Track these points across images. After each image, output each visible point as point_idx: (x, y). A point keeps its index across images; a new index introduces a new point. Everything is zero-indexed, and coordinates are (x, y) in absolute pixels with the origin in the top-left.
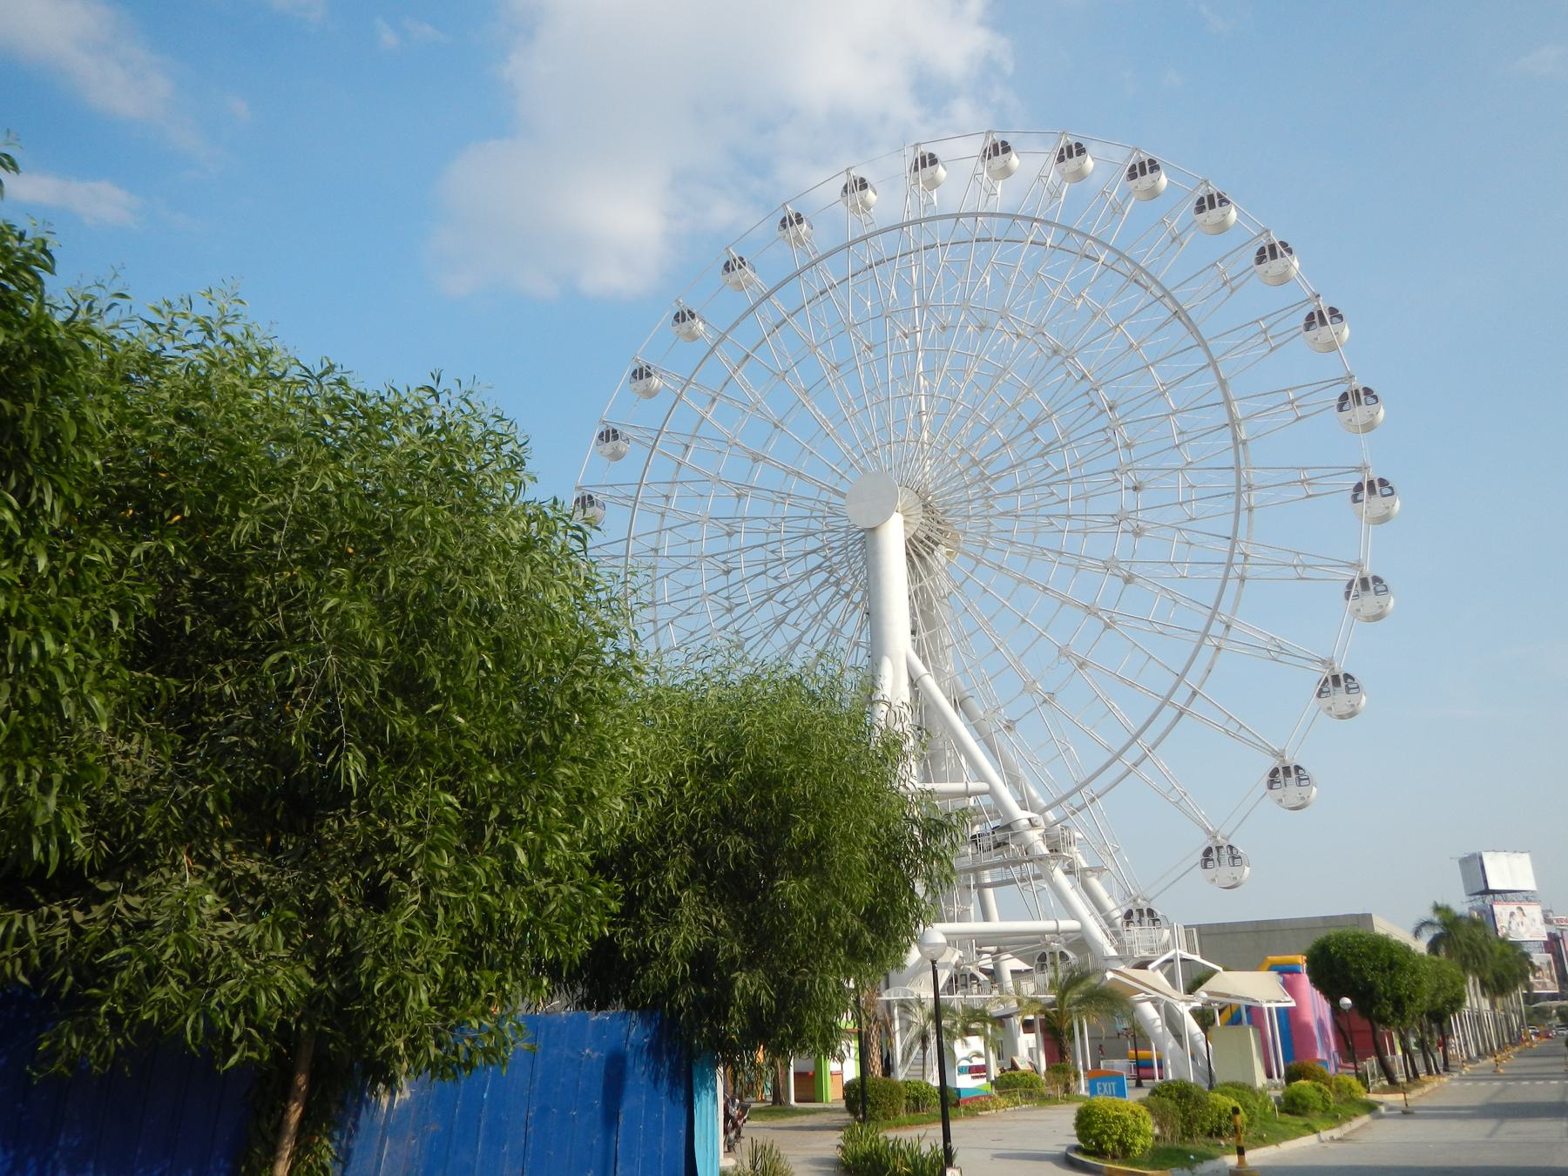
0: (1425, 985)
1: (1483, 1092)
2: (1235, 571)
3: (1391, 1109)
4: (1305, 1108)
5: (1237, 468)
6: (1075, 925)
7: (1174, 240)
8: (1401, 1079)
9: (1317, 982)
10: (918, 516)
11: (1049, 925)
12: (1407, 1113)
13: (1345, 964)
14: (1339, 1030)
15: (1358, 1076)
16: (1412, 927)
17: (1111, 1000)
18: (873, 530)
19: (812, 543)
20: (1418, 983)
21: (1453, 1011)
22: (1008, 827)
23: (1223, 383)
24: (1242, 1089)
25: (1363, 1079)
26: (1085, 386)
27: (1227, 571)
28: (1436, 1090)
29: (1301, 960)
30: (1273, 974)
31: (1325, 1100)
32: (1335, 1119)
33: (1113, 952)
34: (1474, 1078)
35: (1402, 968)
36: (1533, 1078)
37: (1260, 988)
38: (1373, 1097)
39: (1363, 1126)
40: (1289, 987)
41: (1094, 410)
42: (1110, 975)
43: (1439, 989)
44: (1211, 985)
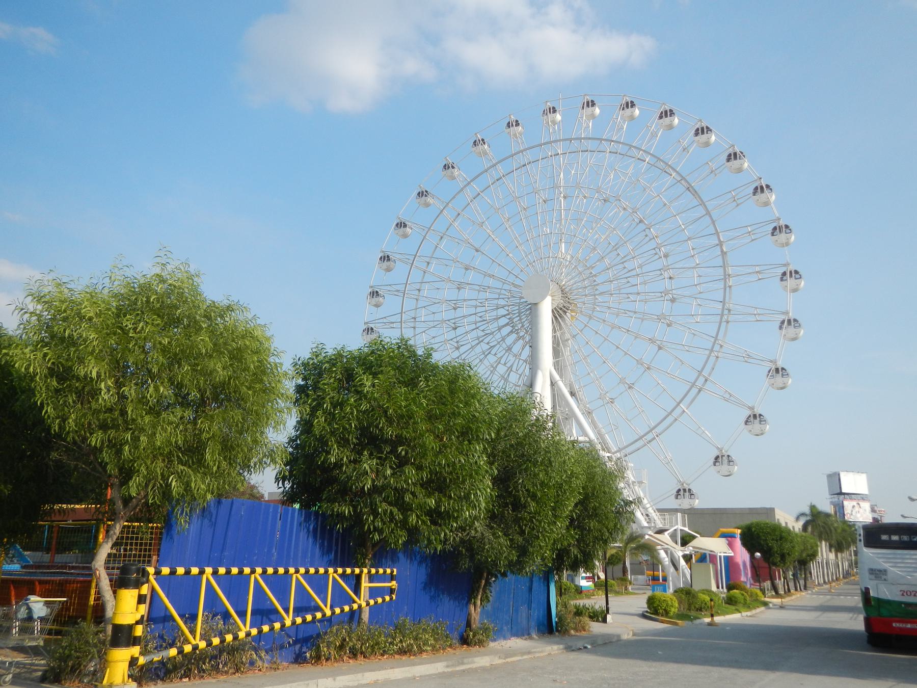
1: (821, 600)
2: (725, 315)
4: (736, 602)
5: (724, 266)
8: (781, 592)
10: (559, 295)
12: (782, 607)
13: (759, 537)
14: (753, 567)
15: (761, 590)
16: (795, 516)
18: (536, 304)
19: (502, 312)
20: (793, 547)
21: (811, 560)
23: (713, 222)
24: (709, 592)
26: (642, 226)
27: (721, 319)
28: (798, 597)
30: (724, 540)
31: (745, 600)
32: (749, 608)
34: (818, 593)
35: (786, 540)
36: (846, 595)
37: (717, 546)
38: (767, 600)
40: (731, 545)
41: (648, 239)
42: (647, 537)
44: (694, 543)
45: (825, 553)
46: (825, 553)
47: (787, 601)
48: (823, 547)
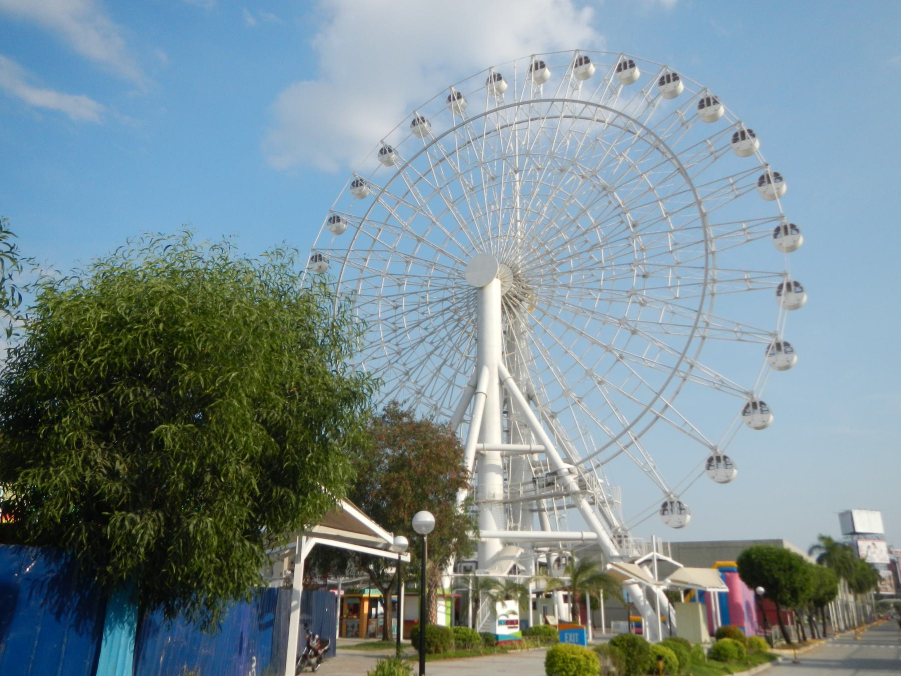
0: (812, 581)
3: (785, 659)
6: (592, 535)
8: (795, 640)
9: (744, 578)
11: (577, 535)
12: (795, 663)
17: (611, 584)
20: (807, 580)
22: (555, 473)
25: (769, 641)
28: (817, 648)
29: (733, 564)
34: (842, 642)
35: (797, 570)
38: (775, 651)
39: (766, 671)
42: (609, 566)
45: (844, 595)
46: (844, 595)
47: (802, 653)
48: (842, 586)
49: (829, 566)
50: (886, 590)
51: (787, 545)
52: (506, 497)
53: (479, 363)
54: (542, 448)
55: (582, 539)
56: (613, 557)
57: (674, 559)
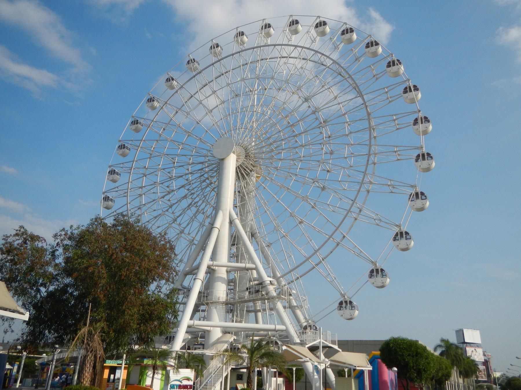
6: (283, 327)
7: (356, 60)
11: (272, 327)
21: (446, 380)
22: (261, 284)
33: (298, 341)
43: (440, 369)
49: (447, 358)
50: (482, 377)
51: (420, 342)
52: (227, 300)
53: (217, 208)
54: (253, 266)
55: (275, 330)
56: (295, 344)
57: (339, 347)
